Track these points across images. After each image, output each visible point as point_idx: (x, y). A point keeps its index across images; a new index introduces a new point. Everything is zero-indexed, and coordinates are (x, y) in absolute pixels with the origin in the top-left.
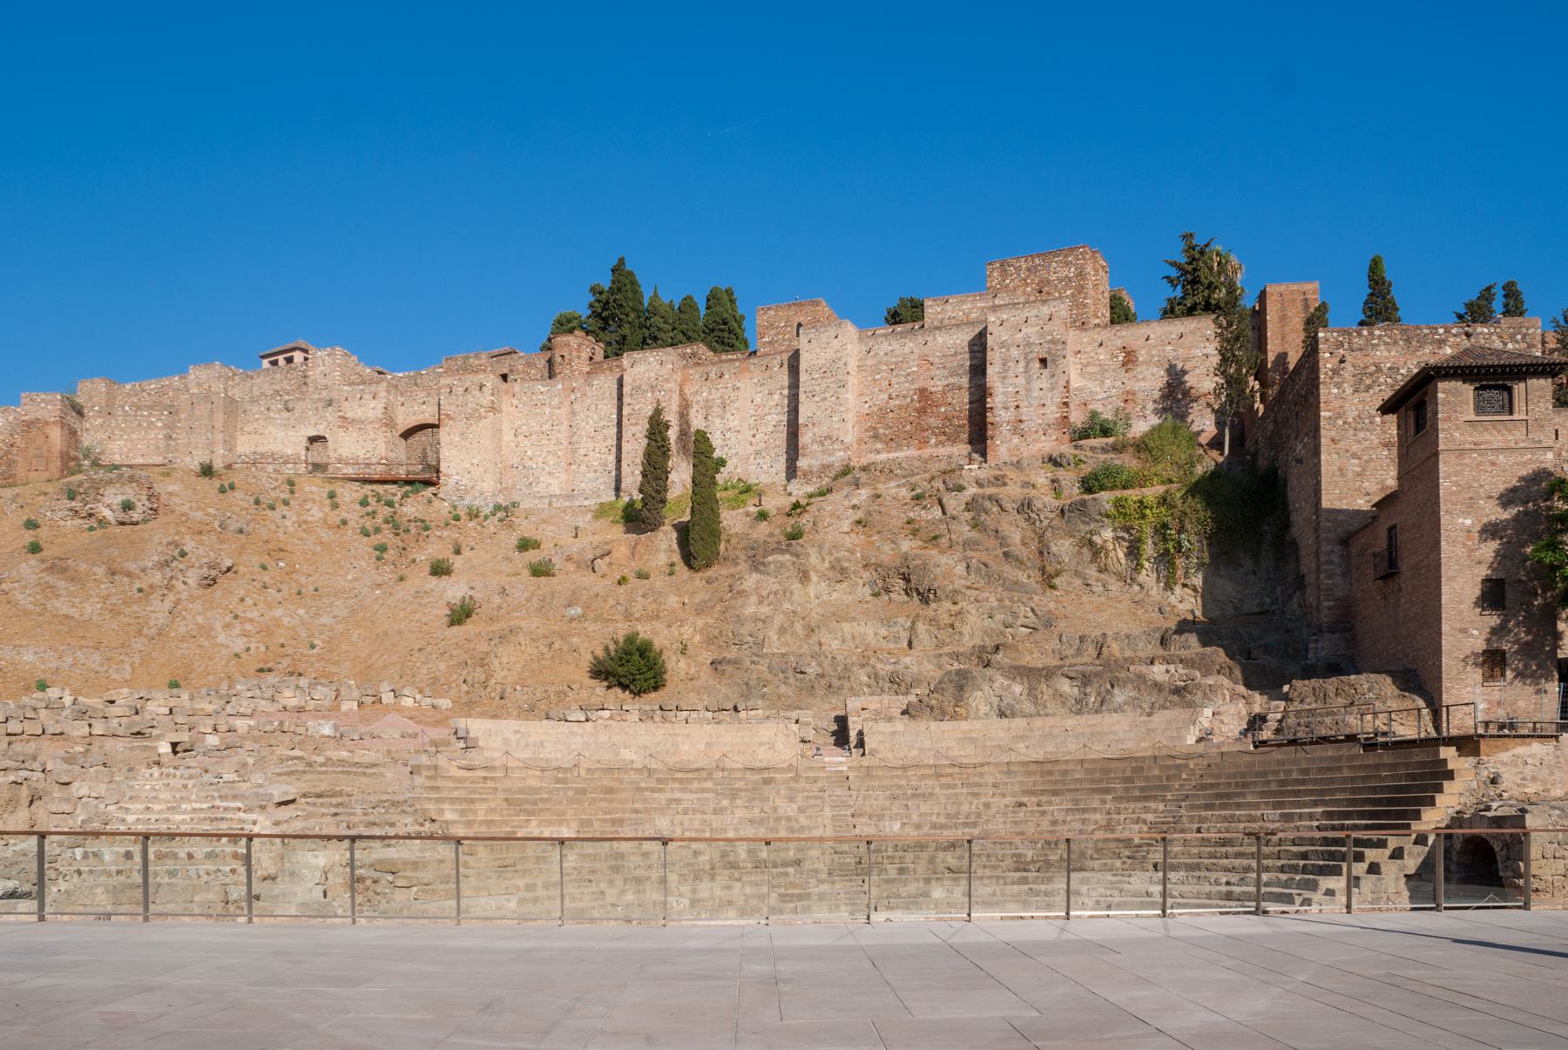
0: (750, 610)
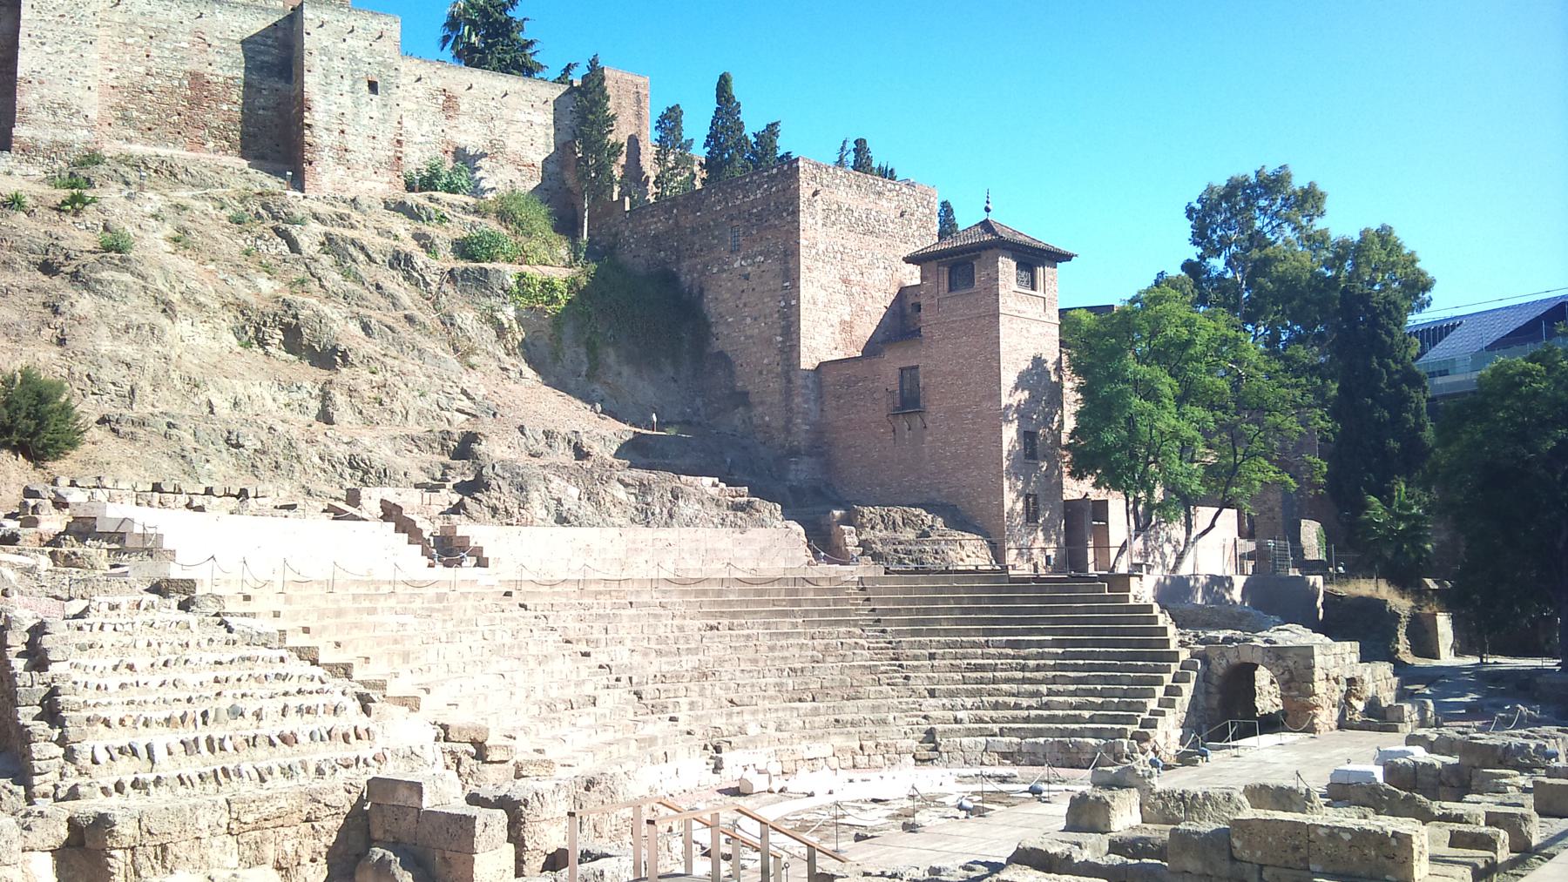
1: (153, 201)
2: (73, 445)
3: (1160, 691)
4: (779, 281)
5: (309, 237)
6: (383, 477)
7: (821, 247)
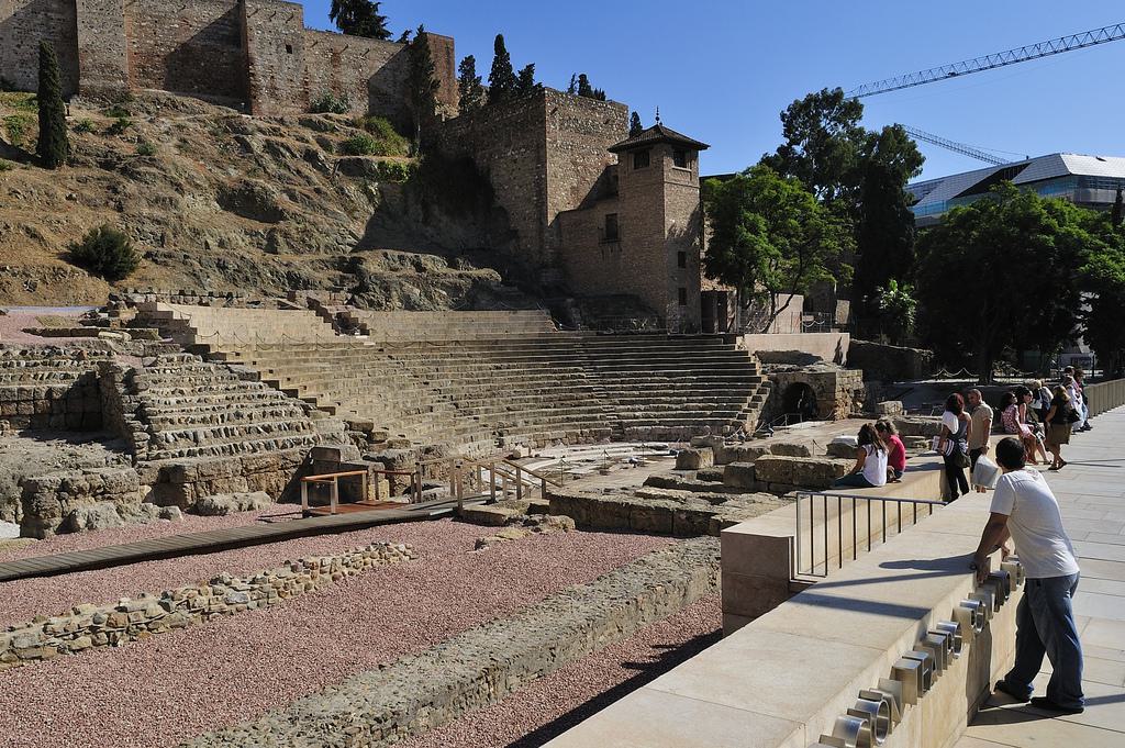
0: (146, 211)
1: (166, 123)
2: (132, 270)
3: (749, 399)
4: (534, 163)
5: (257, 141)
6: (307, 285)
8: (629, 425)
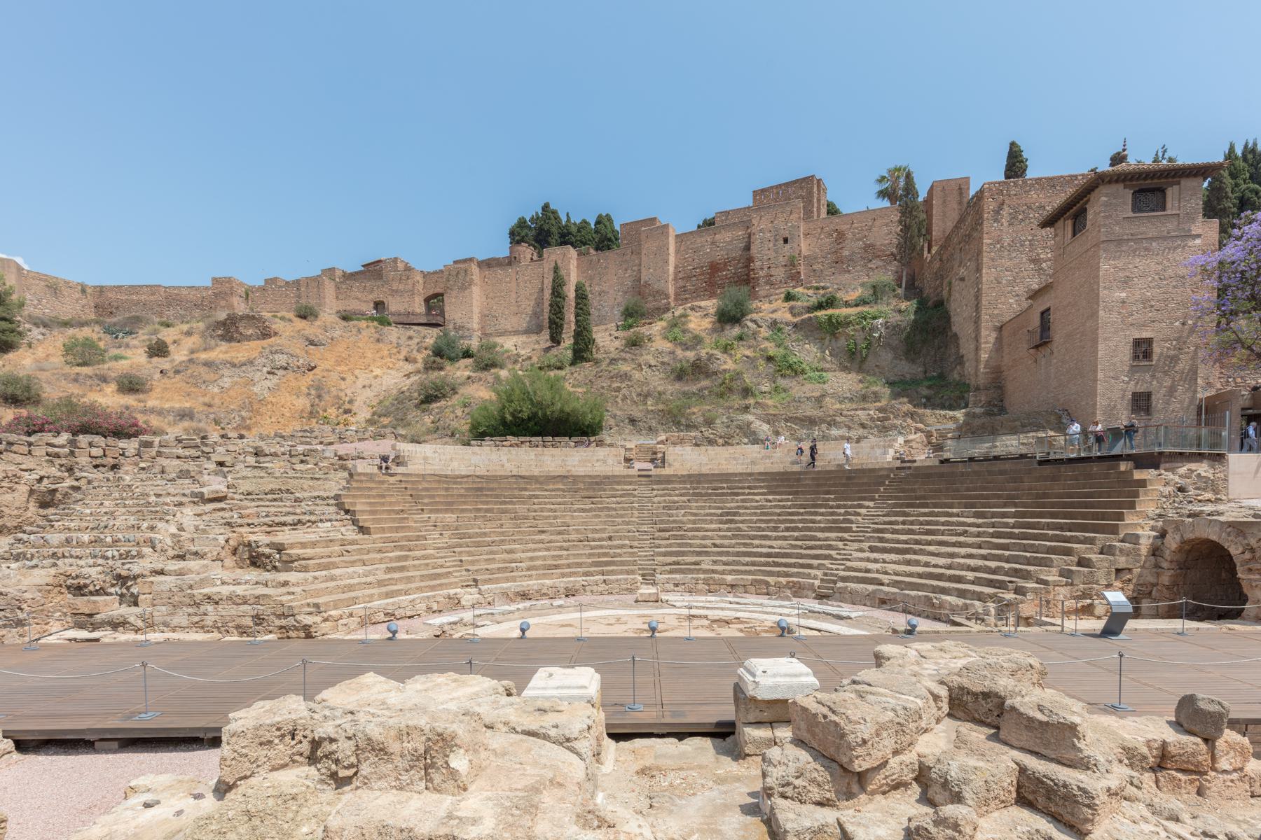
7: (1007, 241)
8: (844, 579)
